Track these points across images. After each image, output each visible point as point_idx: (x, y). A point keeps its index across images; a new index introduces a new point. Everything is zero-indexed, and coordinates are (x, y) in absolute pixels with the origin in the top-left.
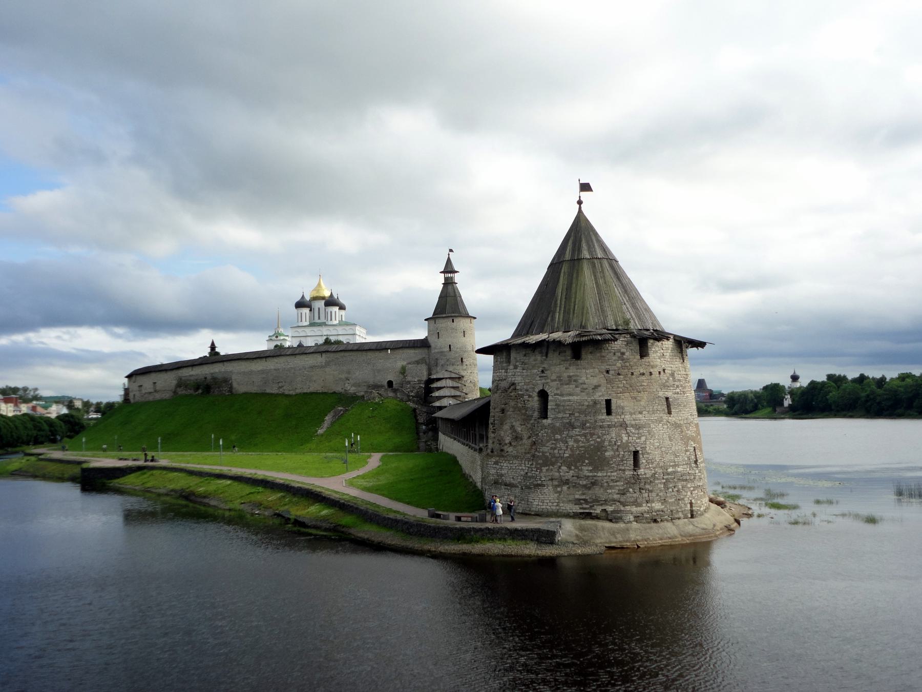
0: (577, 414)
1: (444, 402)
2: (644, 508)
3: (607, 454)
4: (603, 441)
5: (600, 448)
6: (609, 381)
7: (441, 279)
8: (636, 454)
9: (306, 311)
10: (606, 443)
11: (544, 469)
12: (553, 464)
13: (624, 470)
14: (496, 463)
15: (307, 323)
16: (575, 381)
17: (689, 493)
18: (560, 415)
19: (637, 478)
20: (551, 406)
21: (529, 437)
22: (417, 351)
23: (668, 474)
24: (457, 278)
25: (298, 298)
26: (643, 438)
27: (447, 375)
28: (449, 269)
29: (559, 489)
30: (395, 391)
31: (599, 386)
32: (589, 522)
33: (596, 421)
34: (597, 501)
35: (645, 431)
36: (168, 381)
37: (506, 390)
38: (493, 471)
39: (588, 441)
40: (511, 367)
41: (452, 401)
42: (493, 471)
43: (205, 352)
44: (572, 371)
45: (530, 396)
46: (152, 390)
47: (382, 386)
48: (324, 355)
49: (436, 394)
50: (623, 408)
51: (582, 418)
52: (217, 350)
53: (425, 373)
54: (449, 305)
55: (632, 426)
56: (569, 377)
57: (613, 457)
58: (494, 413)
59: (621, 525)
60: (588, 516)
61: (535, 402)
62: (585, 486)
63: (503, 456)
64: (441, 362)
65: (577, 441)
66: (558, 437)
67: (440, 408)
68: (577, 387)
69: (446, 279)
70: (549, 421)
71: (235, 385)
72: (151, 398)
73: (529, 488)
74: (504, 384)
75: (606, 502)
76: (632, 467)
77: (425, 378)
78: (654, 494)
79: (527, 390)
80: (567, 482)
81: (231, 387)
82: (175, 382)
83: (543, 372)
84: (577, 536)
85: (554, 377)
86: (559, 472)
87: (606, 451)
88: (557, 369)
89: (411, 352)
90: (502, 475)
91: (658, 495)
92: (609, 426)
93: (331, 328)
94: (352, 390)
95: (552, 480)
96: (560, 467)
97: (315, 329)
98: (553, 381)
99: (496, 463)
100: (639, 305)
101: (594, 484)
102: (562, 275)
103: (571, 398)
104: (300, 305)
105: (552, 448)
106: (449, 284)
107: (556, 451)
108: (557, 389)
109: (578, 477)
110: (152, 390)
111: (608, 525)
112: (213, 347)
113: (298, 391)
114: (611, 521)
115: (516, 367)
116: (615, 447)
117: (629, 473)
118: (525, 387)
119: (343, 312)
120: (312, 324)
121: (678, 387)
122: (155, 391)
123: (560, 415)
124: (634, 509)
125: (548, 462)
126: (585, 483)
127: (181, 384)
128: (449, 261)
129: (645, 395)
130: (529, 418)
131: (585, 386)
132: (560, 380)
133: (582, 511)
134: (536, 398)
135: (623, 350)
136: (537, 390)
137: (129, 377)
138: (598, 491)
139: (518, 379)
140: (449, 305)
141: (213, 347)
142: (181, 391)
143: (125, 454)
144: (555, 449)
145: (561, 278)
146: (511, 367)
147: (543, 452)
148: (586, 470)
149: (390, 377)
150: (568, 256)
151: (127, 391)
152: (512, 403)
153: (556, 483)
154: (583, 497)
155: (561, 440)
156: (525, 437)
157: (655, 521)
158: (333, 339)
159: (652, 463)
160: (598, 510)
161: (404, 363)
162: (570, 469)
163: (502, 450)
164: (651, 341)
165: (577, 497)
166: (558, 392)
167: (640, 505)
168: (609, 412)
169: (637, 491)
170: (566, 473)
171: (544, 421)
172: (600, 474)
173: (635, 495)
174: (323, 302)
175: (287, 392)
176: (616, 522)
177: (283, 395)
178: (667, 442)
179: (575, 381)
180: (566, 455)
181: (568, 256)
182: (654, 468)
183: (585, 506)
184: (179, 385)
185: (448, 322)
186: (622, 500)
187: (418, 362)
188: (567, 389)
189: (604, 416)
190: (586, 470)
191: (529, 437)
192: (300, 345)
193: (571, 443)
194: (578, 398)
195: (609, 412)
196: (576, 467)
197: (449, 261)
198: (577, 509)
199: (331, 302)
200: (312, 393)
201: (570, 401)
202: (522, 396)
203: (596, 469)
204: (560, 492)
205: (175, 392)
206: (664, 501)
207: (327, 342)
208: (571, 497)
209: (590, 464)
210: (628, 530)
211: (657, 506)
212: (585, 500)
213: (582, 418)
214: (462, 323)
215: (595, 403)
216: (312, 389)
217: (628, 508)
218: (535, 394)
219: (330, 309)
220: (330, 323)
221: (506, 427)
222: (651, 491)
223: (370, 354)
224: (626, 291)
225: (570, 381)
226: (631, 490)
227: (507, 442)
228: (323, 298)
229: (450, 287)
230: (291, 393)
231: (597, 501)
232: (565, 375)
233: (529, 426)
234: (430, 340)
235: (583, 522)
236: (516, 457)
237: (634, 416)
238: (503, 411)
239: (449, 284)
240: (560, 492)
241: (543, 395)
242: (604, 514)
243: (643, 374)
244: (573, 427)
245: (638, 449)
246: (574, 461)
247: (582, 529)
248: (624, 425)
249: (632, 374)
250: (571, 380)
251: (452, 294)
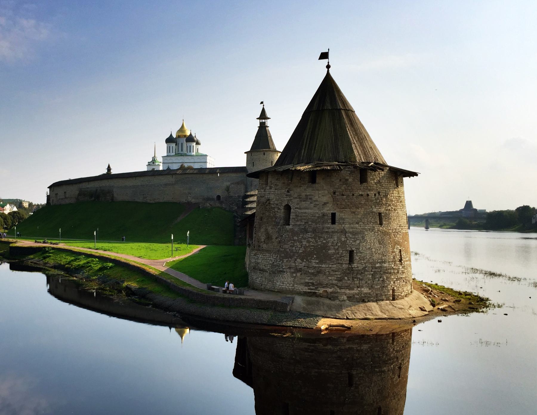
0: (310, 223)
2: (356, 291)
3: (331, 252)
4: (328, 242)
5: (325, 247)
6: (335, 200)
7: (257, 123)
8: (351, 253)
10: (330, 244)
11: (285, 260)
12: (291, 257)
13: (342, 264)
14: (255, 255)
16: (311, 199)
17: (392, 283)
18: (298, 223)
19: (351, 270)
20: (292, 216)
21: (276, 238)
22: (239, 175)
23: (376, 268)
24: (268, 123)
26: (358, 242)
29: (294, 275)
30: (221, 203)
31: (328, 203)
32: (314, 299)
33: (323, 228)
34: (320, 285)
35: (360, 236)
37: (264, 204)
38: (253, 260)
39: (317, 242)
40: (268, 188)
42: (253, 260)
43: (105, 171)
44: (309, 192)
45: (279, 209)
46: (64, 197)
47: (212, 199)
48: (174, 176)
49: (249, 206)
50: (343, 219)
51: (314, 225)
52: (112, 171)
53: (243, 191)
55: (350, 233)
56: (306, 196)
57: (334, 254)
58: (257, 220)
59: (337, 302)
60: (314, 294)
61: (281, 213)
62: (312, 274)
63: (259, 250)
65: (309, 242)
66: (296, 238)
68: (311, 203)
70: (291, 227)
71: (115, 195)
73: (274, 273)
74: (263, 200)
75: (327, 286)
76: (348, 262)
77: (242, 194)
78: (363, 282)
79: (277, 205)
80: (300, 270)
82: (77, 192)
83: (288, 192)
84: (304, 308)
85: (296, 196)
86: (295, 263)
87: (329, 250)
88: (298, 190)
89: (233, 175)
90: (258, 263)
91: (366, 283)
92: (333, 232)
93: (190, 158)
94: (193, 201)
95: (290, 268)
96: (296, 260)
97: (179, 158)
98: (296, 198)
99: (255, 255)
100: (366, 144)
101: (319, 272)
102: (310, 121)
103: (307, 211)
104: (170, 140)
105: (291, 246)
107: (294, 248)
108: (298, 204)
109: (308, 267)
110: (64, 197)
111: (327, 301)
112: (109, 169)
114: (330, 299)
115: (271, 188)
116: (337, 247)
117: (345, 266)
118: (276, 202)
119: (199, 146)
121: (389, 205)
122: (66, 198)
123: (298, 223)
124: (348, 291)
125: (288, 255)
126: (312, 271)
128: (263, 111)
129: (362, 211)
130: (277, 224)
131: (317, 203)
132: (299, 198)
133: (310, 291)
134: (283, 210)
135: (347, 178)
136: (284, 205)
138: (322, 278)
139: (272, 197)
141: (109, 169)
144: (293, 246)
145: (309, 124)
146: (268, 188)
147: (285, 249)
148: (314, 263)
149: (218, 194)
150: (315, 108)
151: (48, 197)
152: (267, 214)
153: (292, 270)
154: (311, 281)
155: (298, 240)
156: (274, 237)
157: (364, 301)
158: (186, 165)
159: (364, 260)
160: (321, 291)
161: (228, 184)
162: (302, 260)
163: (259, 246)
164: (369, 171)
165: (307, 281)
166: (298, 206)
167: (352, 289)
168: (333, 222)
169: (351, 279)
170: (300, 264)
171: (287, 227)
172: (323, 266)
173: (349, 282)
175: (149, 201)
176: (334, 300)
177: (146, 203)
178: (377, 245)
179: (311, 199)
180: (300, 251)
181: (315, 108)
182: (365, 263)
183: (312, 287)
184: (79, 195)
185: (261, 155)
186: (339, 285)
187: (238, 183)
188: (304, 204)
189: (330, 225)
190: (314, 263)
191: (276, 238)
192: (168, 169)
193: (304, 243)
194: (310, 211)
195: (333, 222)
196: (307, 260)
197: (263, 111)
198: (306, 289)
199: (191, 139)
200: (164, 203)
201: (305, 213)
202: (274, 208)
203: (321, 262)
204: (295, 277)
206: (371, 287)
207: (182, 168)
208: (303, 281)
209: (317, 258)
210: (341, 306)
211: (365, 290)
212: (313, 284)
213: (314, 225)
215: (324, 215)
216: (165, 200)
217: (343, 291)
218: (282, 208)
219: (189, 144)
220: (189, 154)
221: (262, 230)
222: (362, 280)
224: (357, 134)
225: (307, 198)
226: (346, 278)
227: (263, 240)
228: (185, 136)
230: (151, 202)
231: (320, 285)
232: (304, 194)
233: (277, 230)
234: (247, 168)
235: (309, 298)
236: (268, 251)
237: (352, 226)
238: (261, 219)
240: (295, 277)
241: (288, 208)
242: (325, 294)
243: (362, 195)
244: (307, 232)
245: (354, 249)
246: (306, 256)
247: (309, 303)
248: (344, 232)
249: (353, 195)
250: (307, 198)
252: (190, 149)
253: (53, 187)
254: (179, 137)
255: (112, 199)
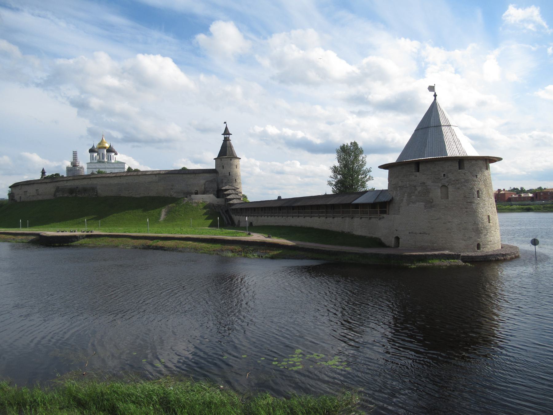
1: (235, 201)
7: (222, 138)
9: (95, 154)
15: (96, 161)
22: (211, 175)
25: (91, 147)
27: (230, 188)
28: (226, 132)
36: (50, 188)
41: (238, 201)
48: (157, 176)
54: (226, 153)
64: (225, 181)
67: (233, 204)
69: (225, 138)
72: (35, 199)
81: (97, 192)
89: (207, 175)
93: (111, 165)
97: (100, 164)
104: (92, 151)
106: (226, 140)
112: (43, 172)
113: (142, 195)
119: (116, 156)
120: (99, 162)
127: (58, 190)
137: (10, 187)
140: (226, 153)
141: (43, 172)
142: (59, 195)
143: (58, 229)
174: (105, 150)
175: (134, 196)
199: (110, 150)
205: (55, 195)
214: (235, 161)
219: (110, 154)
220: (110, 161)
223: (185, 176)
228: (105, 148)
229: (228, 142)
239: (226, 140)
251: (229, 146)
252: (109, 158)
253: (15, 186)
254: (99, 148)
255: (96, 195)
